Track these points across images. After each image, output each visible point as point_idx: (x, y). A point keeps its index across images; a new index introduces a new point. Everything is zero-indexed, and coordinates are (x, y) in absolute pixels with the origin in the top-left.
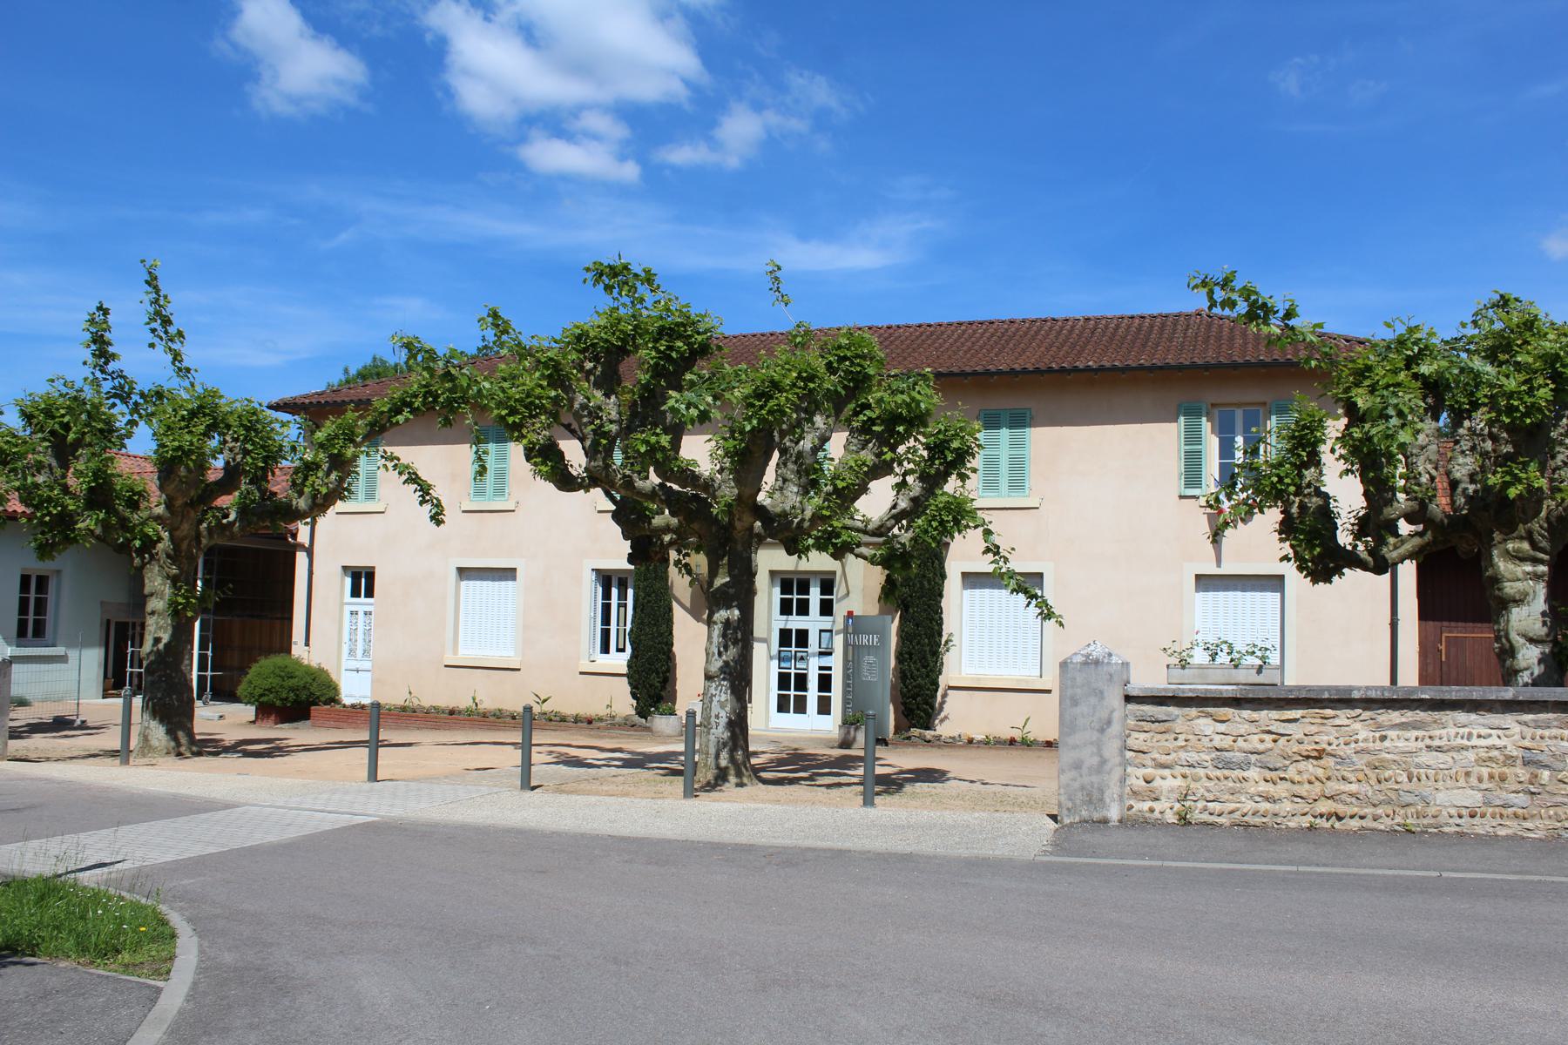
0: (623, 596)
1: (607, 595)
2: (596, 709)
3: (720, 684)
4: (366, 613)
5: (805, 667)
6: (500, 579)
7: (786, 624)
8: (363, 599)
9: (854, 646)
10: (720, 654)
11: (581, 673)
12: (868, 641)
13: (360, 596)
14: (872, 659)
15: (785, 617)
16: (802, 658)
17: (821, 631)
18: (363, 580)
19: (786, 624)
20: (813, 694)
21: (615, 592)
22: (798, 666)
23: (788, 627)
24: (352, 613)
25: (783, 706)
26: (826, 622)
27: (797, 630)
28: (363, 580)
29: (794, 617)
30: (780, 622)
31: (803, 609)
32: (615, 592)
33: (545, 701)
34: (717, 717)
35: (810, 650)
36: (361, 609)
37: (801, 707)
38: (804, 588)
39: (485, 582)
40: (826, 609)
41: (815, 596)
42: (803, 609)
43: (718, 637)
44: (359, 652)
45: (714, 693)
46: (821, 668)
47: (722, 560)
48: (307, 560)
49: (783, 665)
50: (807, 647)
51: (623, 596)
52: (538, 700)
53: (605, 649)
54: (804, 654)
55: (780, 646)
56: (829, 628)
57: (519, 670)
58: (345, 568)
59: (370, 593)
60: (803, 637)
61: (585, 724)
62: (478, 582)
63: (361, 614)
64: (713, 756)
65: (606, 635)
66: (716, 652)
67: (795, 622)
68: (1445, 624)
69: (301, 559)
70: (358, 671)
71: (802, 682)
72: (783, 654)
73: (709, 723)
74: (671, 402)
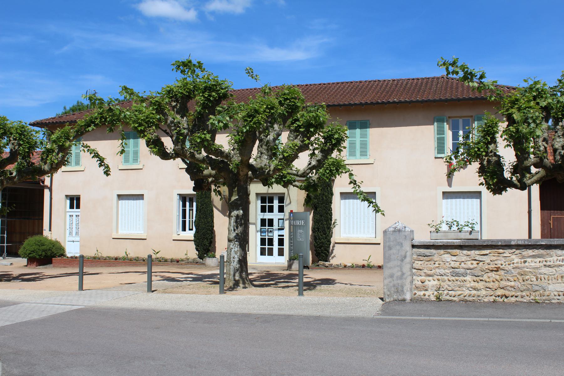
0: (191, 206)
1: (184, 205)
2: (180, 255)
3: (235, 244)
4: (76, 216)
5: (272, 235)
6: (137, 199)
7: (263, 217)
8: (75, 210)
9: (293, 225)
10: (234, 230)
11: (173, 240)
12: (300, 223)
14: (301, 231)
15: (263, 214)
16: (271, 231)
17: (279, 219)
18: (75, 201)
19: (263, 217)
20: (276, 247)
21: (188, 204)
22: (269, 235)
23: (264, 218)
24: (70, 216)
25: (263, 253)
26: (281, 216)
27: (268, 219)
28: (75, 201)
29: (267, 213)
30: (261, 216)
31: (271, 210)
32: (188, 204)
33: (158, 253)
34: (234, 258)
35: (274, 228)
36: (74, 214)
37: (271, 253)
38: (271, 200)
39: (130, 201)
40: (281, 209)
41: (276, 204)
42: (271, 210)
43: (234, 223)
44: (74, 233)
45: (232, 247)
46: (279, 236)
47: (235, 188)
48: (49, 193)
49: (262, 234)
50: (273, 227)
51: (191, 206)
52: (155, 253)
53: (184, 229)
54: (272, 230)
55: (261, 226)
56: (282, 218)
57: (146, 239)
58: (67, 196)
59: (78, 207)
60: (271, 222)
61: (175, 263)
62: (127, 201)
63: (74, 216)
64: (232, 275)
65: (184, 223)
66: (233, 229)
67: (268, 216)
68: (552, 211)
69: (47, 192)
70: (73, 242)
71: (271, 242)
72: (262, 230)
73: (230, 261)
74: (211, 121)
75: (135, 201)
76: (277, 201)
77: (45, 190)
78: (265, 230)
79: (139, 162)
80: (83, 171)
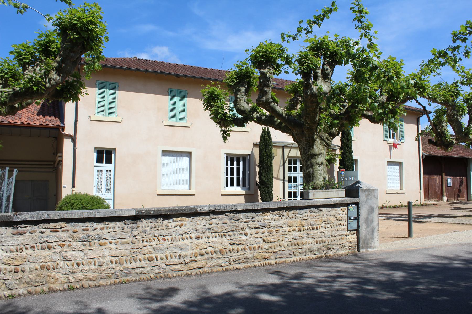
6: (180, 156)
8: (104, 164)
9: (345, 181)
12: (352, 179)
13: (102, 163)
15: (289, 172)
18: (105, 155)
23: (291, 176)
28: (105, 155)
29: (292, 172)
31: (295, 170)
38: (295, 163)
39: (173, 158)
42: (295, 170)
48: (72, 145)
49: (289, 189)
53: (227, 186)
54: (296, 185)
59: (109, 161)
60: (295, 179)
62: (169, 157)
63: (104, 172)
67: (293, 174)
69: (67, 144)
75: (178, 158)
76: (299, 163)
77: (65, 139)
78: (291, 185)
79: (186, 120)
80: (120, 122)
